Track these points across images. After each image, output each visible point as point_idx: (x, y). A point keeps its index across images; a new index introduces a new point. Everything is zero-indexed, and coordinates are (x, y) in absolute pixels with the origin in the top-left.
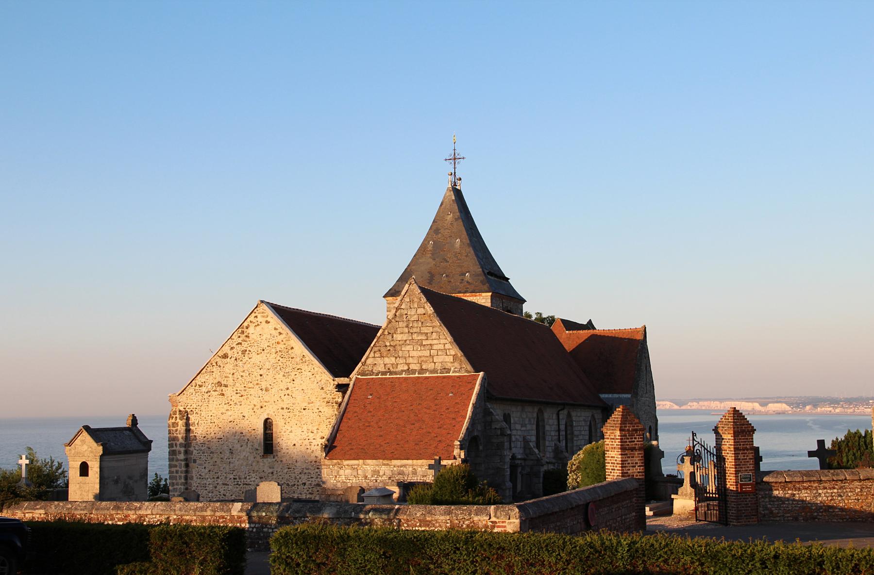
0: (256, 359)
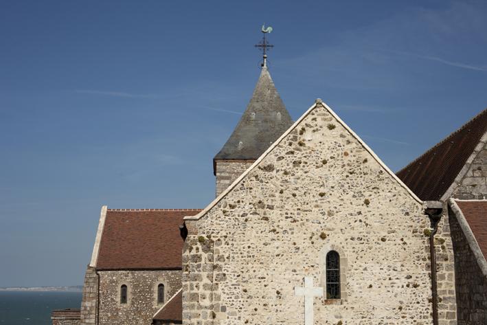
0: (315, 173)
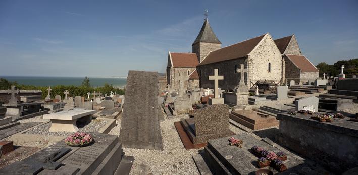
0: (268, 47)
